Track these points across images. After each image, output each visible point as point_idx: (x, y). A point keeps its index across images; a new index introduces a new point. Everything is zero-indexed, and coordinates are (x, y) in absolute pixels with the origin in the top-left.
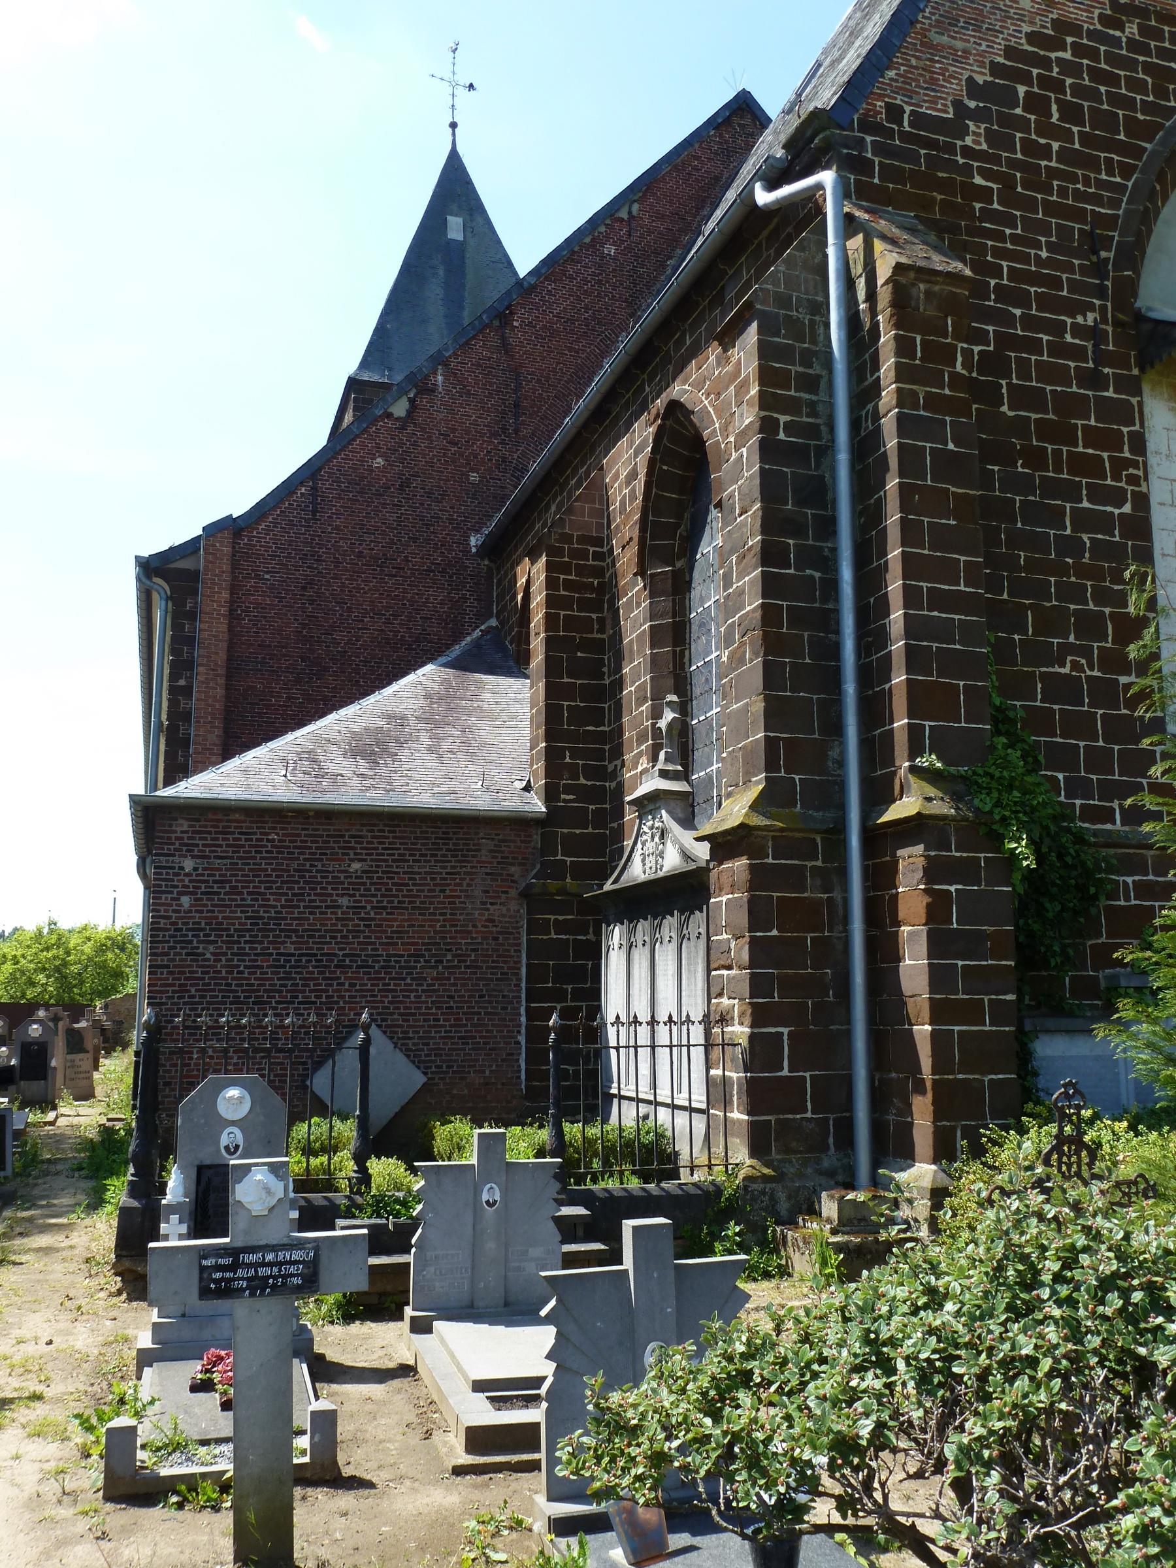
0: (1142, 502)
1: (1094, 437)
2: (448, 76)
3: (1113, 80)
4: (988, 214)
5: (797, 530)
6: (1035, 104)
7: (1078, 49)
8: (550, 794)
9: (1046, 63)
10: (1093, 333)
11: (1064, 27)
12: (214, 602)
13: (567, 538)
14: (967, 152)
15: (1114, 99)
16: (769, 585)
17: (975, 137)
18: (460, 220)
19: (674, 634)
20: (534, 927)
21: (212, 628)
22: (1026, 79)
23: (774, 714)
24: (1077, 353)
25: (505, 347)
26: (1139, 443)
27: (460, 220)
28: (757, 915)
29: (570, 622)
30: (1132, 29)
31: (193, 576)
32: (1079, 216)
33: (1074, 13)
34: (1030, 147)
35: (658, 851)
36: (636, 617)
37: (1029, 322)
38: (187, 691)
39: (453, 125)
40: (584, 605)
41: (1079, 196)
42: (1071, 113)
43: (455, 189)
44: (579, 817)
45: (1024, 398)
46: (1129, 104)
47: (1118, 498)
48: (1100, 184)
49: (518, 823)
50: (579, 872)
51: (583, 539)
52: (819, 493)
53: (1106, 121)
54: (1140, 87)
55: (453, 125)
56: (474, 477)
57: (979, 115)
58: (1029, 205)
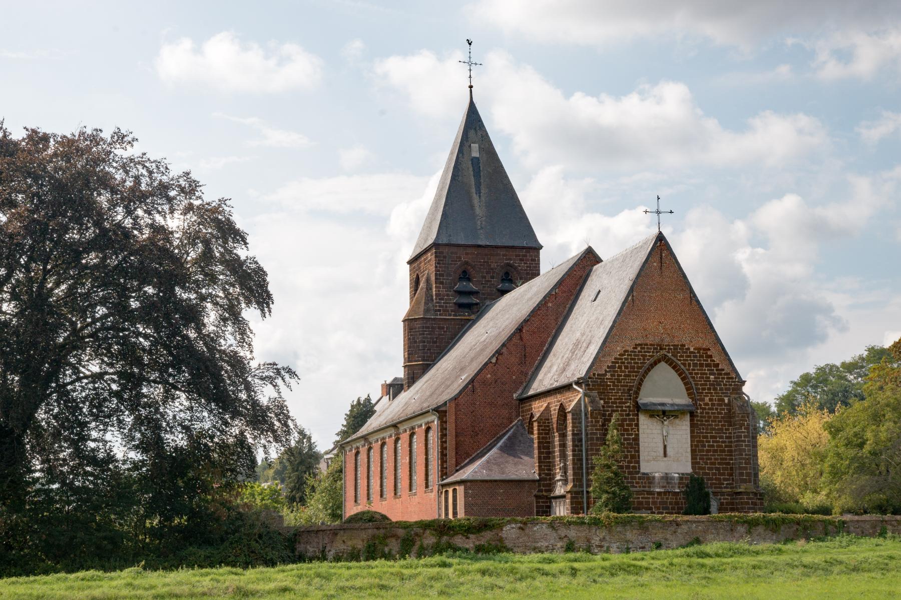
1: (628, 425)
2: (467, 60)
3: (634, 359)
5: (577, 446)
8: (540, 475)
10: (629, 407)
12: (451, 418)
17: (608, 376)
18: (477, 145)
19: (563, 446)
20: (537, 502)
21: (451, 427)
24: (625, 411)
25: (521, 339)
26: (637, 425)
27: (477, 145)
28: (572, 503)
29: (543, 438)
30: (639, 349)
31: (446, 412)
34: (619, 376)
38: (446, 442)
39: (471, 87)
40: (546, 434)
42: (626, 367)
44: (545, 480)
47: (631, 435)
49: (534, 481)
50: (546, 491)
52: (581, 440)
53: (633, 367)
54: (639, 359)
55: (471, 87)
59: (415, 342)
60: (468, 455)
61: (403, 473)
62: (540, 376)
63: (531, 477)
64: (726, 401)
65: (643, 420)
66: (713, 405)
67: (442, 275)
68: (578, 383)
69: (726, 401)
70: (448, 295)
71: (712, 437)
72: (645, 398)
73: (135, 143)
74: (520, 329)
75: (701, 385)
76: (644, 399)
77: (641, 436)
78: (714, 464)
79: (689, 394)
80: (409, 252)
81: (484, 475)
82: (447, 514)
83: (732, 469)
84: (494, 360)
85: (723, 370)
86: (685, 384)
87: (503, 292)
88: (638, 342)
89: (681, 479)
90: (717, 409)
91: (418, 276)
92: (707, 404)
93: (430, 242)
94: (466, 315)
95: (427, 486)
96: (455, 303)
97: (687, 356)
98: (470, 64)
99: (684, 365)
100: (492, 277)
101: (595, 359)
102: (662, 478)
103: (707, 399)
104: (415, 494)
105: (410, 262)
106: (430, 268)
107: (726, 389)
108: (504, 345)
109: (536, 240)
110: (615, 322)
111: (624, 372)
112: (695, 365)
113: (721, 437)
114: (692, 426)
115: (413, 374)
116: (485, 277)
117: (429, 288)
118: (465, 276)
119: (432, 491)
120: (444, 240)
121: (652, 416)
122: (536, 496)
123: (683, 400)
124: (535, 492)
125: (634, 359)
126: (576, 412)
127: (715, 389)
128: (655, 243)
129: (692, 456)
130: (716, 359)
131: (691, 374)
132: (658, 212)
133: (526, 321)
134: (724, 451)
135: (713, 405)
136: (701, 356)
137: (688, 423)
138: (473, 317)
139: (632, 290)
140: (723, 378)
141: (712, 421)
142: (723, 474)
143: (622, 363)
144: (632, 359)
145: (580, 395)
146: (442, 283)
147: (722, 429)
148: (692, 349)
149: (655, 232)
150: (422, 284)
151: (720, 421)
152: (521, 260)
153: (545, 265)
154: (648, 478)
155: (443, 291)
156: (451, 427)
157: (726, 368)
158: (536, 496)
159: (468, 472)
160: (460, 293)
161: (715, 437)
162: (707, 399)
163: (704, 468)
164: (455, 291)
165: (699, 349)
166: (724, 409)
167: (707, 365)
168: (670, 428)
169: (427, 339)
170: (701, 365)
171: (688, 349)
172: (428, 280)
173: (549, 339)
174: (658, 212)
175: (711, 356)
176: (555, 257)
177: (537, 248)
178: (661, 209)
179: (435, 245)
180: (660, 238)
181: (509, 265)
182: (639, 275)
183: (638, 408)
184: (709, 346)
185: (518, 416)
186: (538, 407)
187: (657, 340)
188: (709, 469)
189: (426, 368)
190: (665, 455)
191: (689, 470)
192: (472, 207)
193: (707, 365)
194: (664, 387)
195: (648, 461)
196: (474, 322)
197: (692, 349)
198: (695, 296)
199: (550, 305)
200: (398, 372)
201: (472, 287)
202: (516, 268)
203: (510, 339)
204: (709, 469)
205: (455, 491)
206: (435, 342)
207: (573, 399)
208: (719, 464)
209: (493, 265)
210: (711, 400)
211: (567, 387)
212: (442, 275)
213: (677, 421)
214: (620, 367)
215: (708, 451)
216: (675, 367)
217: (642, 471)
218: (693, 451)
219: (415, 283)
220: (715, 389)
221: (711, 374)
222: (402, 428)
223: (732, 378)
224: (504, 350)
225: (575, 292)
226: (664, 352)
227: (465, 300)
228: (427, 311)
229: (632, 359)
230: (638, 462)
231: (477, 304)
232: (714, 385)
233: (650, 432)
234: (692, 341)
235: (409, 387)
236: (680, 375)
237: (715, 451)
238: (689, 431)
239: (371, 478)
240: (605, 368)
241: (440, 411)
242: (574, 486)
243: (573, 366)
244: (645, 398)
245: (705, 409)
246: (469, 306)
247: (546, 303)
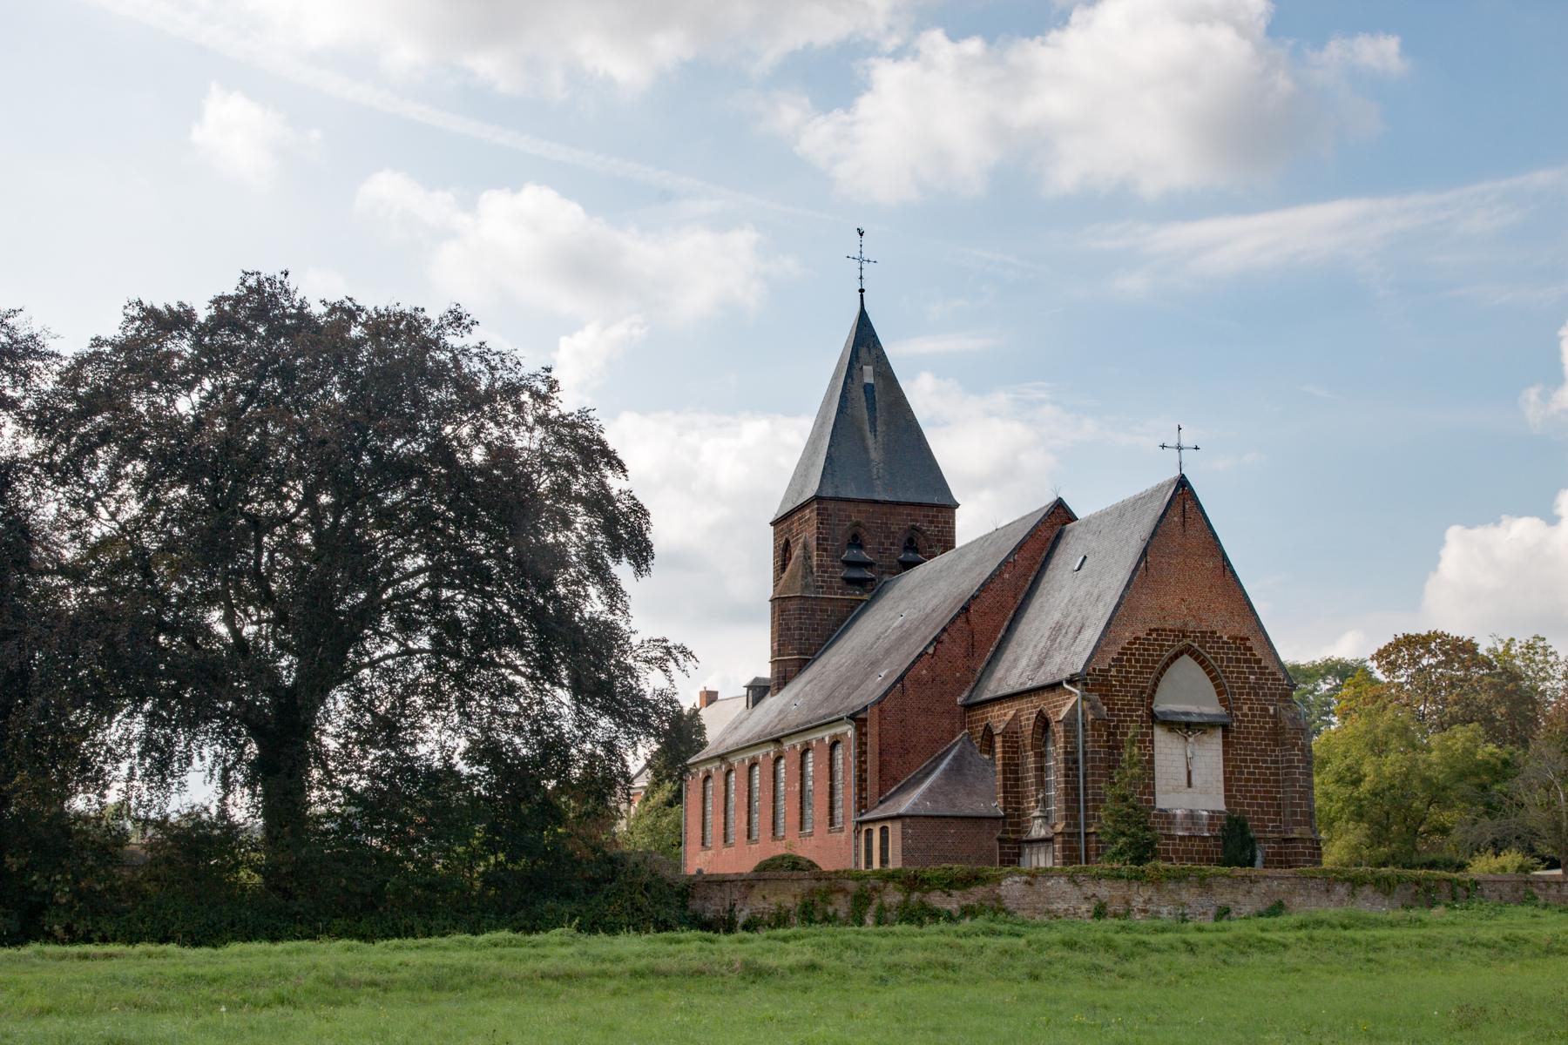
0: (1152, 756)
2: (857, 255)
8: (1005, 810)
12: (872, 730)
16: (1066, 782)
17: (1113, 672)
19: (1042, 769)
21: (872, 741)
23: (1068, 809)
25: (968, 621)
26: (1152, 742)
28: (1064, 849)
35: (1037, 830)
36: (1031, 761)
39: (862, 291)
42: (1137, 661)
43: (865, 338)
49: (997, 818)
50: (1014, 832)
52: (1076, 761)
53: (1147, 661)
55: (862, 291)
60: (896, 780)
61: (788, 807)
62: (999, 672)
63: (992, 813)
65: (1160, 734)
66: (1254, 716)
67: (825, 539)
71: (1252, 761)
72: (1165, 704)
73: (474, 328)
74: (965, 609)
76: (1162, 705)
77: (1157, 757)
78: (1254, 798)
79: (1221, 701)
80: (774, 510)
81: (928, 808)
82: (869, 862)
83: (1279, 806)
84: (931, 651)
86: (1216, 686)
87: (908, 565)
89: (1211, 818)
91: (787, 542)
92: (1245, 715)
93: (810, 492)
94: (856, 594)
95: (832, 823)
96: (843, 578)
98: (861, 260)
99: (1215, 659)
100: (892, 544)
101: (1096, 647)
102: (1186, 816)
103: (1245, 708)
104: (811, 834)
105: (774, 523)
106: (808, 532)
108: (944, 630)
109: (951, 496)
110: (1122, 597)
112: (1230, 660)
113: (1265, 761)
114: (1227, 744)
115: (784, 674)
116: (881, 544)
117: (807, 558)
118: (856, 542)
119: (841, 830)
121: (1171, 730)
122: (999, 839)
123: (1211, 707)
124: (998, 834)
126: (1070, 723)
127: (1256, 694)
128: (1176, 490)
130: (1258, 654)
132: (1179, 448)
133: (974, 598)
134: (1268, 781)
135: (1254, 716)
137: (1220, 741)
138: (866, 597)
139: (1145, 553)
142: (1268, 813)
145: (1073, 700)
146: (825, 550)
150: (797, 552)
152: (931, 522)
153: (970, 524)
154: (1167, 816)
155: (827, 560)
156: (872, 741)
158: (999, 839)
159: (907, 803)
160: (849, 564)
161: (1257, 761)
162: (1245, 708)
163: (1242, 805)
165: (1235, 638)
167: (1246, 661)
169: (804, 629)
170: (1238, 660)
172: (805, 547)
174: (1179, 448)
175: (1250, 649)
176: (983, 516)
177: (948, 507)
178: (1183, 444)
179: (817, 498)
180: (1182, 483)
181: (913, 528)
182: (1153, 534)
183: (1154, 719)
184: (1248, 634)
185: (963, 728)
186: (1000, 717)
187: (1179, 624)
188: (1249, 805)
189: (803, 665)
190: (1189, 784)
191: (1223, 807)
192: (866, 450)
193: (1246, 661)
194: (1187, 690)
195: (1167, 792)
196: (869, 604)
198: (1229, 564)
199: (1006, 576)
200: (764, 670)
201: (866, 556)
202: (923, 533)
203: (953, 621)
204: (1249, 805)
205: (884, 830)
207: (1063, 707)
209: (894, 528)
210: (1251, 709)
211: (1054, 687)
212: (825, 539)
213: (1205, 737)
214: (1129, 660)
215: (1248, 780)
216: (1202, 663)
217: (1158, 806)
218: (1226, 780)
219: (783, 554)
220: (1256, 694)
222: (787, 745)
224: (945, 637)
225: (1040, 560)
226: (1188, 641)
227: (856, 574)
228: (806, 587)
230: (1153, 794)
231: (872, 580)
233: (1168, 751)
234: (1226, 627)
235: (779, 690)
236: (1209, 673)
237: (1257, 780)
239: (731, 813)
241: (857, 719)
242: (1068, 825)
243: (1058, 659)
244: (1165, 704)
246: (861, 583)
247: (1001, 574)
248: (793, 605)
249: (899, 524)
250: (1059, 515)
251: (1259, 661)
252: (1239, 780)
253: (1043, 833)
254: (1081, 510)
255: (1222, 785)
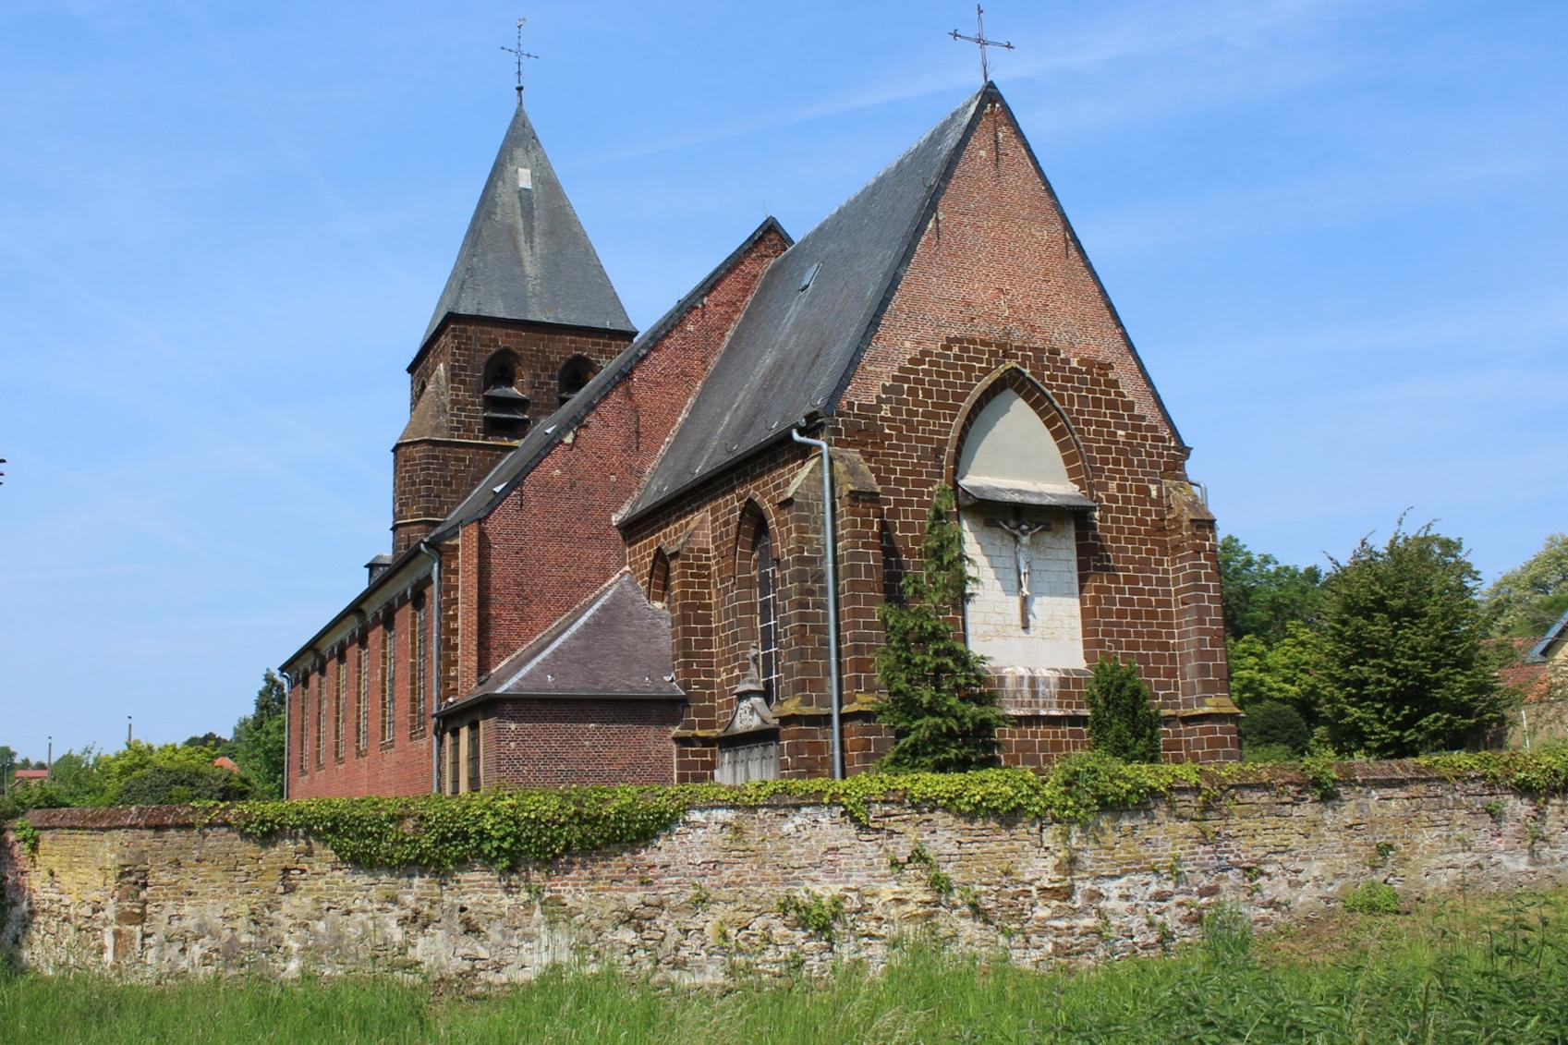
2: (515, 48)
3: (945, 375)
4: (891, 446)
6: (912, 392)
7: (932, 363)
8: (686, 686)
9: (917, 372)
11: (925, 353)
13: (691, 550)
14: (882, 419)
15: (948, 384)
17: (886, 411)
18: (528, 171)
20: (681, 754)
22: (907, 380)
25: (629, 396)
30: (956, 349)
32: (931, 441)
33: (929, 346)
34: (911, 413)
37: (908, 493)
38: (455, 617)
39: (520, 89)
40: (701, 585)
41: (931, 432)
42: (928, 394)
45: (906, 527)
46: (953, 385)
48: (941, 425)
50: (703, 726)
51: (700, 550)
54: (957, 376)
55: (520, 89)
56: (613, 478)
57: (887, 401)
58: (909, 439)
59: (414, 484)
60: (508, 649)
63: (665, 692)
64: (1154, 494)
66: (1127, 500)
67: (464, 369)
68: (813, 426)
69: (1154, 494)
70: (473, 404)
71: (1128, 580)
75: (1099, 450)
79: (1071, 473)
83: (1173, 657)
84: (569, 439)
85: (1143, 418)
86: (1062, 447)
88: (954, 333)
89: (1064, 682)
90: (1135, 511)
92: (1113, 499)
97: (1065, 379)
98: (519, 53)
99: (1060, 398)
100: (552, 377)
103: (1113, 485)
105: (411, 369)
107: (1154, 465)
111: (925, 404)
113: (1148, 581)
120: (467, 308)
122: (677, 740)
125: (945, 375)
127: (1129, 463)
128: (981, 107)
129: (1084, 624)
131: (1076, 421)
134: (1152, 615)
135: (1127, 500)
136: (1096, 382)
137: (1072, 544)
140: (1144, 438)
141: (1128, 541)
143: (917, 381)
144: (940, 374)
146: (463, 382)
147: (1145, 562)
148: (1074, 363)
149: (979, 84)
151: (1143, 542)
157: (1148, 414)
162: (1113, 485)
164: (486, 398)
165: (1089, 363)
166: (1148, 513)
167: (1111, 404)
168: (1034, 554)
171: (1067, 361)
173: (691, 401)
175: (1114, 384)
178: (987, 36)
187: (997, 331)
191: (1081, 664)
192: (520, 262)
193: (1111, 404)
197: (1074, 363)
199: (691, 328)
206: (448, 484)
208: (1147, 646)
210: (1121, 488)
212: (464, 369)
213: (1047, 538)
215: (1121, 614)
216: (1039, 403)
220: (1129, 463)
221: (1119, 426)
223: (1162, 439)
226: (1011, 364)
229: (940, 374)
232: (1131, 449)
236: (1049, 424)
237: (1136, 615)
238: (1074, 565)
240: (877, 391)
245: (1109, 509)
248: (418, 452)
249: (560, 351)
250: (770, 234)
251: (1129, 406)
252: (1108, 613)
253: (754, 722)
254: (798, 231)
255: (1078, 623)
